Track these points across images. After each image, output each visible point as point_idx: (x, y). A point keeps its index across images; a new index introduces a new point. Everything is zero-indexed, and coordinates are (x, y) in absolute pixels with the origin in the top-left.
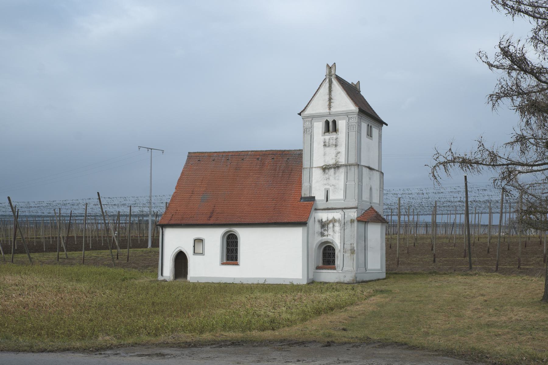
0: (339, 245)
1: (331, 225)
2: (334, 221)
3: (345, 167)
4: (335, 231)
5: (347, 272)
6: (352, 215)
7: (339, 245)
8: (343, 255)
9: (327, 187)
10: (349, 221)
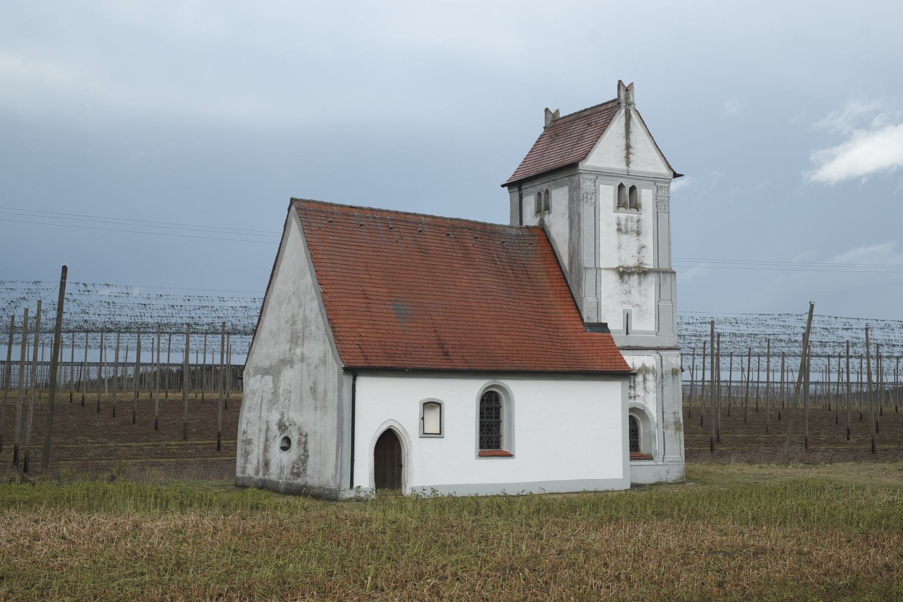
0: (654, 414)
1: (640, 378)
2: (645, 370)
3: (656, 274)
4: (647, 389)
5: (671, 463)
6: (673, 361)
7: (654, 414)
8: (664, 432)
9: (627, 307)
10: (669, 371)
